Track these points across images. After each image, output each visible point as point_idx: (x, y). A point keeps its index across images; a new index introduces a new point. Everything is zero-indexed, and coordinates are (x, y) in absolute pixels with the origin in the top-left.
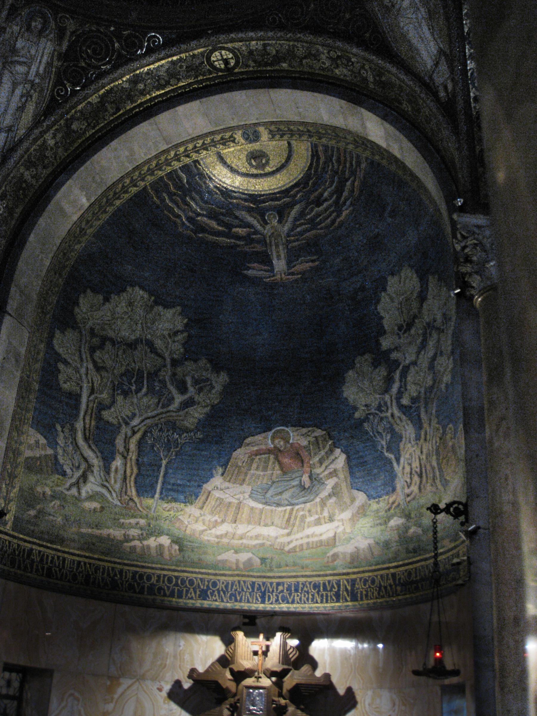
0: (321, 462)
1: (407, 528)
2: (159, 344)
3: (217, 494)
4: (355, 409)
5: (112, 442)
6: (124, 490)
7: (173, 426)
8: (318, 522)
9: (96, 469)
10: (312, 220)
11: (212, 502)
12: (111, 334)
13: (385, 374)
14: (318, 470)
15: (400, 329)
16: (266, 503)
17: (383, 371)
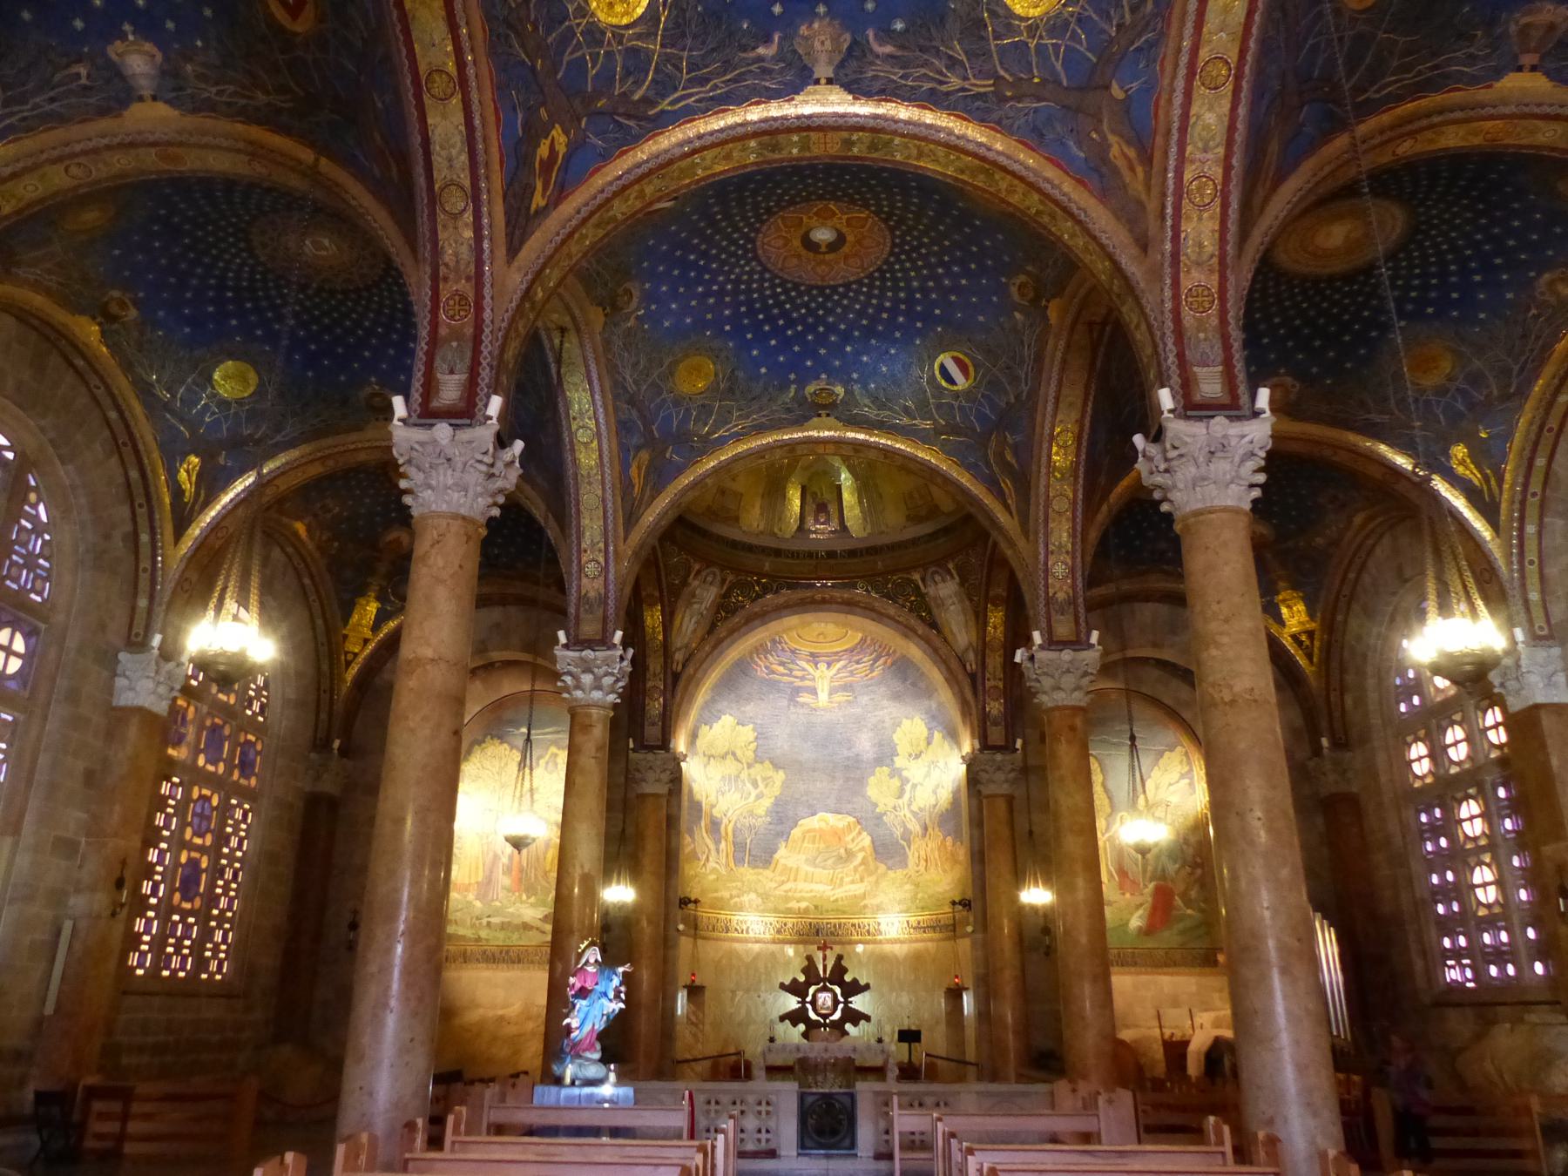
0: (853, 840)
1: (917, 893)
2: (739, 753)
3: (782, 861)
4: (876, 805)
5: (718, 831)
6: (727, 865)
7: (751, 814)
8: (853, 882)
9: (713, 853)
10: (851, 672)
11: (780, 867)
12: (713, 752)
13: (898, 784)
14: (850, 846)
15: (910, 755)
16: (816, 867)
17: (896, 782)
